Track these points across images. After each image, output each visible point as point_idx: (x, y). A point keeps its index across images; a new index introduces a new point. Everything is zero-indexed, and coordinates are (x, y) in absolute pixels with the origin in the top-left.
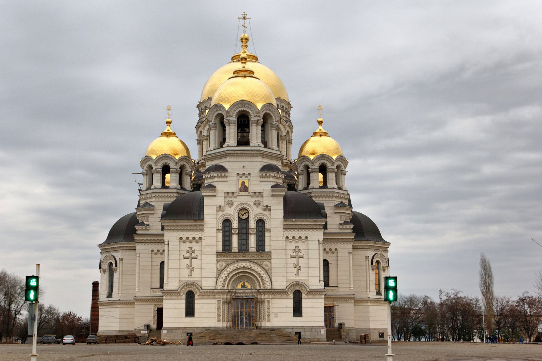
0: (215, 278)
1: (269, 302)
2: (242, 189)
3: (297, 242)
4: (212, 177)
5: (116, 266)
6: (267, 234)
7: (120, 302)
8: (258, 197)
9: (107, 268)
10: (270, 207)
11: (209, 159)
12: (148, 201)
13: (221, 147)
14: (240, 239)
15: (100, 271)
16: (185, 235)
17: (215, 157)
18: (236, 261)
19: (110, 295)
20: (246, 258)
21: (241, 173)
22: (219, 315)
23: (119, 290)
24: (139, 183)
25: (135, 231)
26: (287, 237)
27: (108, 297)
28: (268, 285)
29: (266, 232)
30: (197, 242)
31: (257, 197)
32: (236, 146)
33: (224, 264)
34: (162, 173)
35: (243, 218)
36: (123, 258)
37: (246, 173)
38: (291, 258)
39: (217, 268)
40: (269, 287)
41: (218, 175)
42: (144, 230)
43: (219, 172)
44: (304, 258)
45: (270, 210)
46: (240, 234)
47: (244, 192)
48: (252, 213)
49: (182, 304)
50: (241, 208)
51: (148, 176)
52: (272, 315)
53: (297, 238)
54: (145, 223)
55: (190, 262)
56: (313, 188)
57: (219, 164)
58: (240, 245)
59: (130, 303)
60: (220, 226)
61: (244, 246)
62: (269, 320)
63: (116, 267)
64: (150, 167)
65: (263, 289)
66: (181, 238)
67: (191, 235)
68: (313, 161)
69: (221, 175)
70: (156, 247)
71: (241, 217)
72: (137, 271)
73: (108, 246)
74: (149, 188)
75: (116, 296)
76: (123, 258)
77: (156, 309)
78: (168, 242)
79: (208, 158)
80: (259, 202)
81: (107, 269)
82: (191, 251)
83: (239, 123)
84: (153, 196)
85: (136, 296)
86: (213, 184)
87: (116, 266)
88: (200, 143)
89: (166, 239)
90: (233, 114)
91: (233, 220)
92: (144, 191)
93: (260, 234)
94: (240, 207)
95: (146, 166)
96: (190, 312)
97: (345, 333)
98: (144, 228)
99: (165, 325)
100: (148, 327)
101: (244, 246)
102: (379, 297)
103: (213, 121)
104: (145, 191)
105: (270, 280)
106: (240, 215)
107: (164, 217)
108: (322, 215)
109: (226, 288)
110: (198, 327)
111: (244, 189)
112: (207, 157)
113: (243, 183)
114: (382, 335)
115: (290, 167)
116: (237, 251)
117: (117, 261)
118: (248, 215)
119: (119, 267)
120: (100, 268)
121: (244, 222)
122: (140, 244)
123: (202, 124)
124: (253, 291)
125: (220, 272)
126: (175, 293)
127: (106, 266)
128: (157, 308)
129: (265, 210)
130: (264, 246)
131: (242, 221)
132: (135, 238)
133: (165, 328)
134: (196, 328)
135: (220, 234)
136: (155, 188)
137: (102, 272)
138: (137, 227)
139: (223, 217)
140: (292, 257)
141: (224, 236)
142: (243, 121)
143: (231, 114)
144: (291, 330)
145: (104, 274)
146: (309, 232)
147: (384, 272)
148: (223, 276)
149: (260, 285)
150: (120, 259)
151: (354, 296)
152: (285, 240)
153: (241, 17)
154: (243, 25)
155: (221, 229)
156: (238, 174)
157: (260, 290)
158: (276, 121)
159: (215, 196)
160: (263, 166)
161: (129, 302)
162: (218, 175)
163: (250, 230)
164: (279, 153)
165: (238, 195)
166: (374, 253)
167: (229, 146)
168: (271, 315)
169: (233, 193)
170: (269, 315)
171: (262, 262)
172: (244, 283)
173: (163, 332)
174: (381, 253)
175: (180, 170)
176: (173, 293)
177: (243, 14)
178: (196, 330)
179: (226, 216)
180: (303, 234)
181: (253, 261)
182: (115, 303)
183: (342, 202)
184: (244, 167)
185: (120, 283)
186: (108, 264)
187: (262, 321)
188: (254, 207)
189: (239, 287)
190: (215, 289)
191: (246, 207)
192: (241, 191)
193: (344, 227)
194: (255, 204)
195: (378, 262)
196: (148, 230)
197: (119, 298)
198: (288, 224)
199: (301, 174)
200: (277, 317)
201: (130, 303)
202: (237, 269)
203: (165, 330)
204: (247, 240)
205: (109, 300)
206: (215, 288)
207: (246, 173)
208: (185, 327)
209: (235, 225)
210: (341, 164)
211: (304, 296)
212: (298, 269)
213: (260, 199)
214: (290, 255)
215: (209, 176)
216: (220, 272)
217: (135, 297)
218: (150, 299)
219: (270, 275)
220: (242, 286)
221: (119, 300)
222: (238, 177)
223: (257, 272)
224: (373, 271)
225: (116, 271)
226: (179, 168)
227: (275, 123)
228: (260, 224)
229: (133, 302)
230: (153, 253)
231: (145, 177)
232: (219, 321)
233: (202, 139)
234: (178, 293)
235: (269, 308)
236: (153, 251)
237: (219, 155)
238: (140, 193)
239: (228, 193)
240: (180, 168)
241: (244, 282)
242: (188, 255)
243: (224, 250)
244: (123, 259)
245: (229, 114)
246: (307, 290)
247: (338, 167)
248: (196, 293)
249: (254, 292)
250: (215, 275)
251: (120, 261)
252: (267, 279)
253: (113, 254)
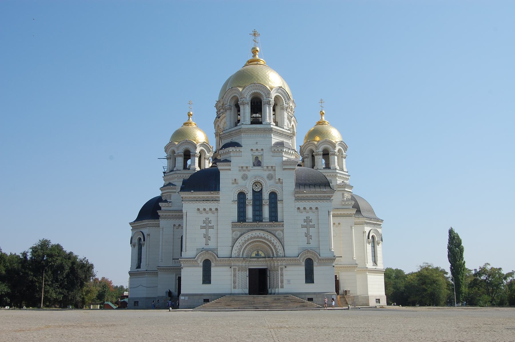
0: (231, 246)
1: (282, 269)
3: (308, 212)
4: (228, 152)
5: (144, 240)
6: (279, 205)
7: (147, 272)
8: (271, 171)
9: (136, 242)
10: (282, 180)
11: (224, 137)
12: (171, 181)
13: (236, 125)
14: (254, 210)
15: (131, 246)
16: (202, 205)
17: (230, 135)
18: (250, 230)
19: (139, 267)
20: (260, 228)
21: (254, 149)
22: (235, 282)
23: (146, 261)
24: (163, 167)
25: (160, 208)
26: (299, 208)
27: (137, 268)
28: (281, 253)
29: (279, 203)
30: (214, 213)
31: (270, 170)
32: (250, 124)
33: (239, 234)
34: (183, 156)
35: (256, 191)
36: (150, 234)
37: (260, 149)
38: (302, 228)
39: (233, 237)
40: (281, 255)
41: (233, 150)
43: (234, 148)
44: (314, 228)
45: (282, 183)
46: (254, 205)
47: (257, 166)
48: (265, 185)
49: (199, 271)
50: (255, 182)
51: (171, 160)
52: (285, 282)
53: (308, 209)
54: (168, 201)
55: (207, 232)
56: (318, 169)
57: (234, 141)
58: (254, 215)
59: (154, 273)
60: (236, 198)
61: (258, 217)
62: (282, 287)
63: (144, 242)
64: (174, 152)
65: (276, 257)
66: (198, 209)
67: (207, 205)
68: (317, 145)
69: (236, 150)
70: (177, 222)
71: (254, 190)
72: (160, 244)
73: (137, 223)
74: (172, 170)
75: (143, 267)
76: (150, 234)
77: (177, 278)
79: (223, 136)
80: (272, 176)
81: (136, 244)
82: (207, 221)
83: (253, 104)
84: (176, 177)
85: (159, 266)
86: (228, 159)
87: (144, 240)
88: (218, 136)
89: (184, 211)
90: (246, 96)
91: (247, 192)
92: (167, 173)
93: (273, 205)
94: (254, 180)
95: (169, 151)
96: (207, 279)
97: (350, 299)
98: (167, 205)
99: (183, 292)
100: (170, 293)
101: (258, 217)
102: (375, 267)
103: (228, 104)
104: (169, 172)
105: (282, 248)
106: (253, 188)
107: (183, 189)
108: (331, 188)
109: (241, 256)
110: (214, 294)
111: (258, 163)
112: (223, 136)
113: (257, 158)
114: (378, 301)
115: (296, 155)
116: (251, 221)
117: (145, 237)
118: (261, 188)
119: (147, 242)
120: (131, 243)
121: (258, 195)
122: (163, 219)
123: (219, 118)
124: (266, 259)
125: (235, 241)
126: (193, 261)
127: (136, 241)
128: (178, 277)
129: (277, 183)
130: (276, 217)
131: (256, 194)
132: (159, 214)
133: (183, 294)
134: (212, 295)
135: (236, 206)
136: (177, 170)
137: (132, 246)
138: (160, 204)
139: (238, 190)
140: (303, 226)
141: (239, 208)
142: (256, 102)
143: (245, 96)
144: (303, 296)
145: (134, 248)
146: (319, 203)
147: (378, 245)
148: (237, 244)
149: (273, 253)
150: (147, 234)
151: (356, 265)
152: (297, 211)
153: (253, 33)
154: (253, 40)
155: (236, 201)
156: (252, 150)
157: (273, 258)
158: (286, 104)
159: (230, 170)
160: (275, 142)
161: (155, 272)
162: (233, 150)
163: (263, 202)
164: (289, 132)
165: (252, 169)
166: (370, 228)
167: (242, 124)
168: (284, 282)
169: (247, 167)
170: (282, 282)
171: (275, 232)
172: (258, 252)
173: (181, 299)
174: (376, 228)
175: (200, 154)
176: (192, 261)
177: (254, 31)
178: (212, 296)
179: (241, 189)
180: (313, 204)
181: (266, 230)
182: (142, 274)
183: (343, 182)
184: (257, 143)
185: (147, 256)
186: (138, 239)
187: (276, 288)
188: (266, 180)
189: (254, 255)
190: (231, 257)
191: (260, 180)
192: (254, 165)
193: (346, 203)
194: (268, 177)
195: (373, 237)
196: (170, 206)
197: (146, 269)
198: (299, 195)
199: (307, 158)
200: (290, 284)
201: (154, 273)
202: (252, 238)
203: (183, 296)
204: (261, 212)
205: (138, 271)
206: (230, 257)
207: (260, 149)
208: (201, 294)
209: (250, 196)
210: (342, 149)
211: (315, 263)
212: (309, 238)
213: (272, 172)
214: (302, 225)
215: (225, 152)
216: (235, 241)
217: (159, 267)
218: (172, 269)
219: (283, 244)
220: (256, 254)
221: (146, 270)
222: (252, 153)
223: (270, 242)
224: (369, 244)
225: (144, 245)
226: (199, 153)
227: (285, 105)
228: (273, 196)
229: (157, 272)
230: (174, 227)
231: (169, 160)
232: (235, 287)
233: (219, 132)
234: (196, 261)
235: (282, 275)
236: (174, 225)
237: (234, 133)
238: (164, 175)
239: (242, 167)
240: (200, 153)
241: (258, 251)
242: (205, 225)
243: (239, 221)
244: (150, 234)
245: (243, 95)
246: (318, 258)
247: (339, 150)
248: (213, 261)
249: (267, 260)
250: (230, 244)
251: (147, 236)
252: (280, 248)
253: (141, 230)
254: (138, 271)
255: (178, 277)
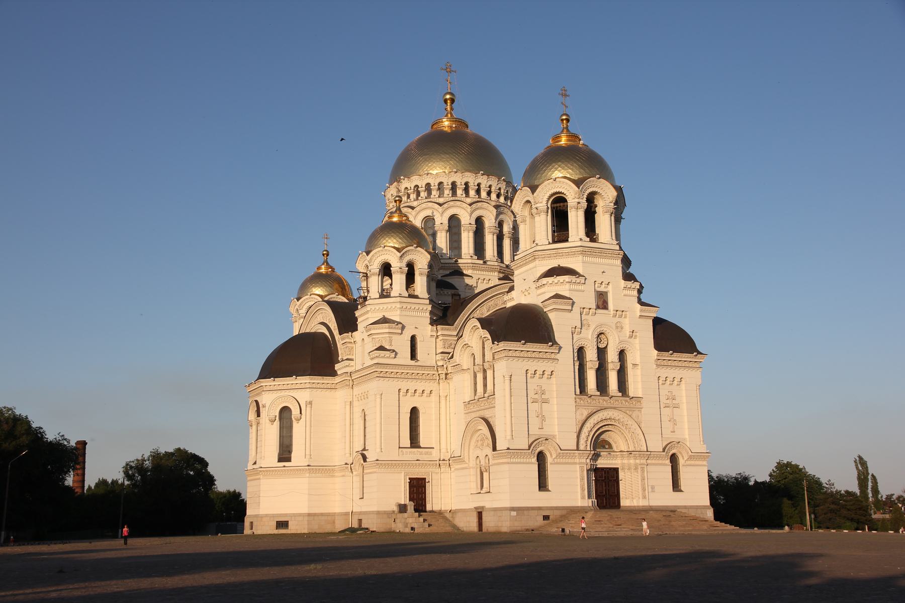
2: (600, 303)
5: (301, 413)
16: (532, 365)
42: (387, 357)
61: (602, 386)
67: (540, 366)
78: (511, 376)
101: (602, 386)
118: (606, 343)
121: (602, 353)
128: (410, 479)
205: (284, 467)
209: (591, 356)
221: (308, 466)
254: (284, 467)
255: (408, 479)
